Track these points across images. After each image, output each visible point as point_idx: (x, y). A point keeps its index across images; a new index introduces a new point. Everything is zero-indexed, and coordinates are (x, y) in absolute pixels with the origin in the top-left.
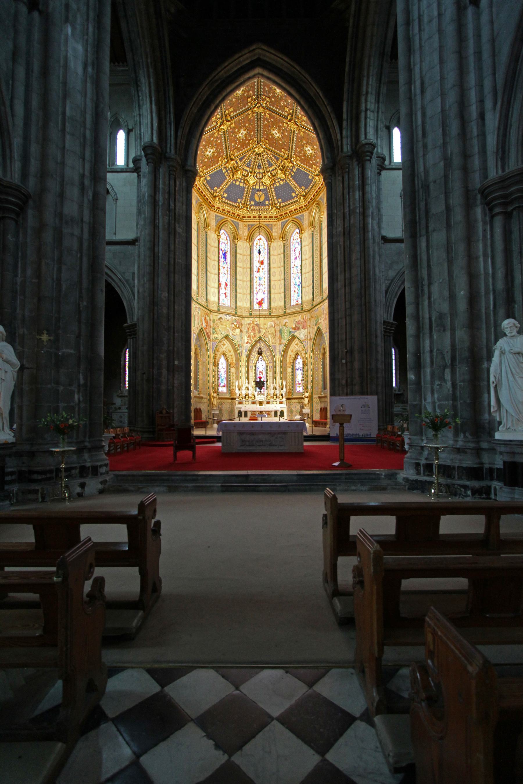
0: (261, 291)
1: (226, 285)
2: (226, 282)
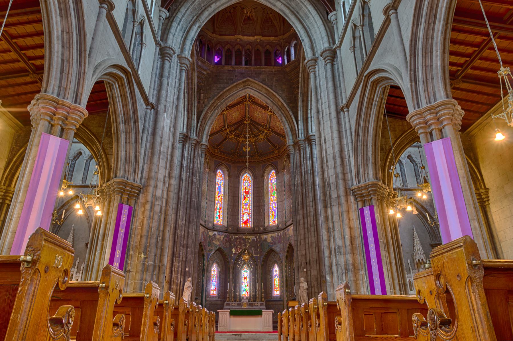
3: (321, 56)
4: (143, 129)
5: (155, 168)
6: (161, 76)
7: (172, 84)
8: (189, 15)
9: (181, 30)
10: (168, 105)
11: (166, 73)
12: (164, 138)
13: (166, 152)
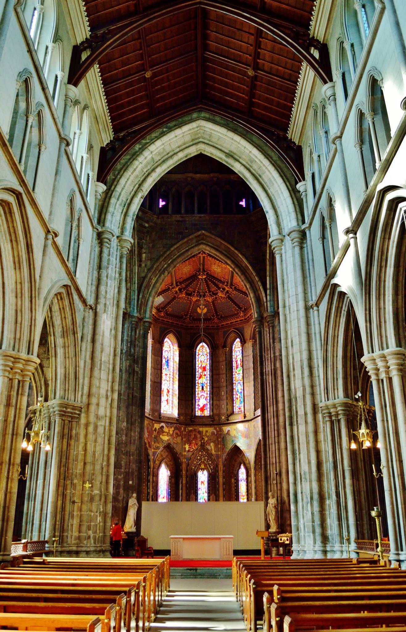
0: (203, 397)
1: (168, 392)
2: (168, 389)
3: (289, 235)
4: (82, 337)
5: (95, 382)
6: (100, 267)
7: (111, 276)
8: (130, 185)
9: (121, 205)
10: (108, 303)
11: (104, 263)
12: (104, 345)
13: (107, 361)
